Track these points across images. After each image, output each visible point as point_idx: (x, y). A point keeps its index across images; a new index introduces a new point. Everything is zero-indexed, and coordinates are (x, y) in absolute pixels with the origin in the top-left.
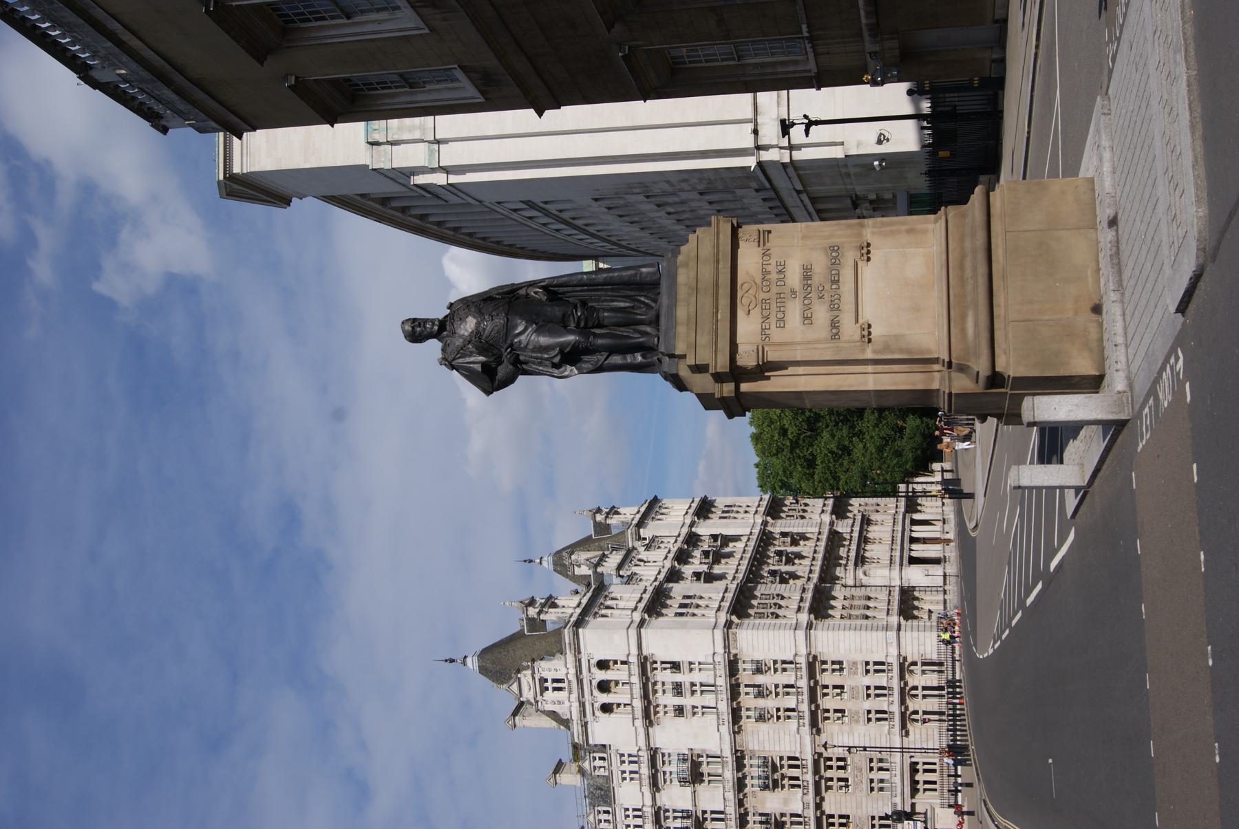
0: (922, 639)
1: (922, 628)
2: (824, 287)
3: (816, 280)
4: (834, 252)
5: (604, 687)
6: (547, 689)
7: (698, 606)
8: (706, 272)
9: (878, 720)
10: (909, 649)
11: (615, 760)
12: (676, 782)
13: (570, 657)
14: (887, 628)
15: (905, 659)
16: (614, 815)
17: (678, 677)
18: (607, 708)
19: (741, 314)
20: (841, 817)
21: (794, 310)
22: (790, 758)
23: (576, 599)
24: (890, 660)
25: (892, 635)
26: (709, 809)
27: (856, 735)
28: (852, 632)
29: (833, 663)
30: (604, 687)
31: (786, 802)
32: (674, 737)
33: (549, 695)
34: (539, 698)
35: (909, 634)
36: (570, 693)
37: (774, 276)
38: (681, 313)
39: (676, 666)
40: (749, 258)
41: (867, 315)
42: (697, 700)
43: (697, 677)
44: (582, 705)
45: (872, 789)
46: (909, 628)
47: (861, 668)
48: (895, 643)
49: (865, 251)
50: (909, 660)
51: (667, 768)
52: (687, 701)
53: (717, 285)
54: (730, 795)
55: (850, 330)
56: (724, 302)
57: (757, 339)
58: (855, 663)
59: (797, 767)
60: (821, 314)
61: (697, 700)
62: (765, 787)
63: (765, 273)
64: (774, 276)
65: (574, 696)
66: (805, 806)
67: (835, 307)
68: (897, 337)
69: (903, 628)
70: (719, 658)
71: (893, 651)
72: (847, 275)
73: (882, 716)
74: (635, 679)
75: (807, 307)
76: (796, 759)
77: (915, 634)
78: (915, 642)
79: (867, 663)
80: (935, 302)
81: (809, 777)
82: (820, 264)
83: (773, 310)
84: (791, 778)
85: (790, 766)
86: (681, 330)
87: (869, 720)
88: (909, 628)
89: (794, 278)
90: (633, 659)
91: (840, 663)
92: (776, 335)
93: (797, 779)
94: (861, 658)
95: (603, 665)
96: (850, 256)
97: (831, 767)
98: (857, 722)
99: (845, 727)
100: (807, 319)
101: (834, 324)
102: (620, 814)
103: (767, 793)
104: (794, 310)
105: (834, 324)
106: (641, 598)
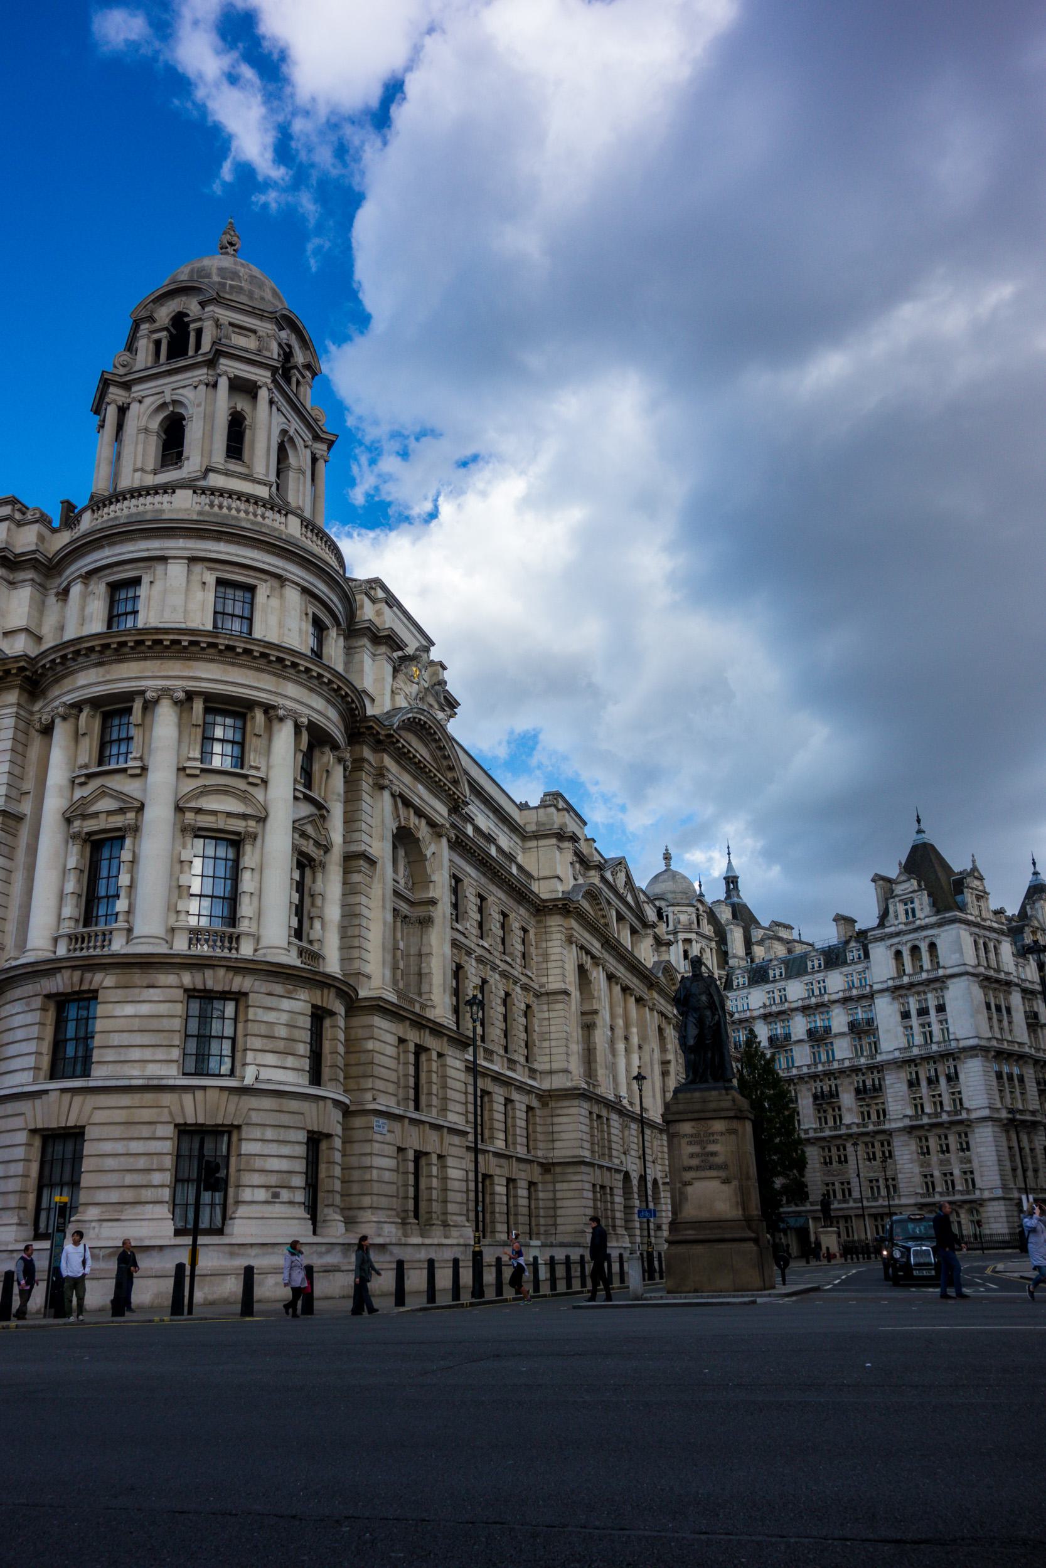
0: (1000, 1220)
1: (1011, 1219)
2: (707, 1163)
3: (711, 1159)
4: (723, 1167)
5: (915, 949)
6: (906, 904)
7: (1000, 1021)
8: (713, 1105)
9: (926, 1183)
10: (990, 1209)
11: (860, 967)
12: (851, 1018)
13: (933, 919)
14: (1004, 1187)
15: (981, 1205)
16: (818, 971)
17: (933, 1012)
18: (898, 954)
19: (693, 1123)
20: (845, 1156)
21: (695, 1149)
22: (884, 1111)
23: (991, 916)
24: (978, 1192)
25: (999, 1193)
26: (835, 1047)
27: (910, 1166)
28: (995, 1158)
29: (967, 1143)
30: (915, 949)
31: (850, 1110)
32: (885, 1011)
33: (901, 908)
34: (897, 899)
35: (1003, 1208)
36: (905, 924)
37: (711, 1138)
38: (697, 1094)
39: (941, 1008)
40: (719, 1126)
41: (698, 1185)
42: (917, 1029)
43: (936, 1028)
44: (898, 934)
45: (871, 1181)
46: (1010, 1208)
47: (966, 1166)
48: (992, 1196)
49: (726, 1181)
50: (981, 1209)
51: (859, 1010)
52: (915, 1021)
53: (703, 1111)
54: (847, 1064)
55: (688, 1176)
56: (696, 1116)
57: (682, 1132)
58: (970, 1161)
59: (879, 1117)
60: (695, 1162)
61: (917, 1029)
62: (858, 1091)
63: (713, 1134)
64: (711, 1138)
65: (902, 927)
66: (848, 1126)
67: (698, 1168)
68: (687, 1199)
69: (1008, 1202)
70: (954, 1044)
71: (987, 1195)
72: (714, 1173)
73: (930, 1187)
74: (924, 976)
75: (698, 1155)
76: (885, 1116)
77: (1003, 1214)
78: (996, 1214)
79: (972, 1172)
80: (704, 1215)
81: (871, 1128)
82: (718, 1160)
83: (695, 1139)
84: (826, 1118)
85: (878, 1111)
86: (689, 1095)
87: (925, 1176)
88: (1010, 1208)
89: (711, 1148)
90: (941, 972)
91: (968, 1149)
92: (684, 1141)
93: (869, 1118)
94: (975, 1165)
95: (932, 946)
96: (723, 1174)
97: (882, 1145)
98: (922, 1166)
99: (915, 1156)
100: (692, 1156)
101: (690, 1168)
102: (819, 976)
103: (853, 1094)
104: (695, 1149)
105: (690, 1168)
106: (665, 1063)
